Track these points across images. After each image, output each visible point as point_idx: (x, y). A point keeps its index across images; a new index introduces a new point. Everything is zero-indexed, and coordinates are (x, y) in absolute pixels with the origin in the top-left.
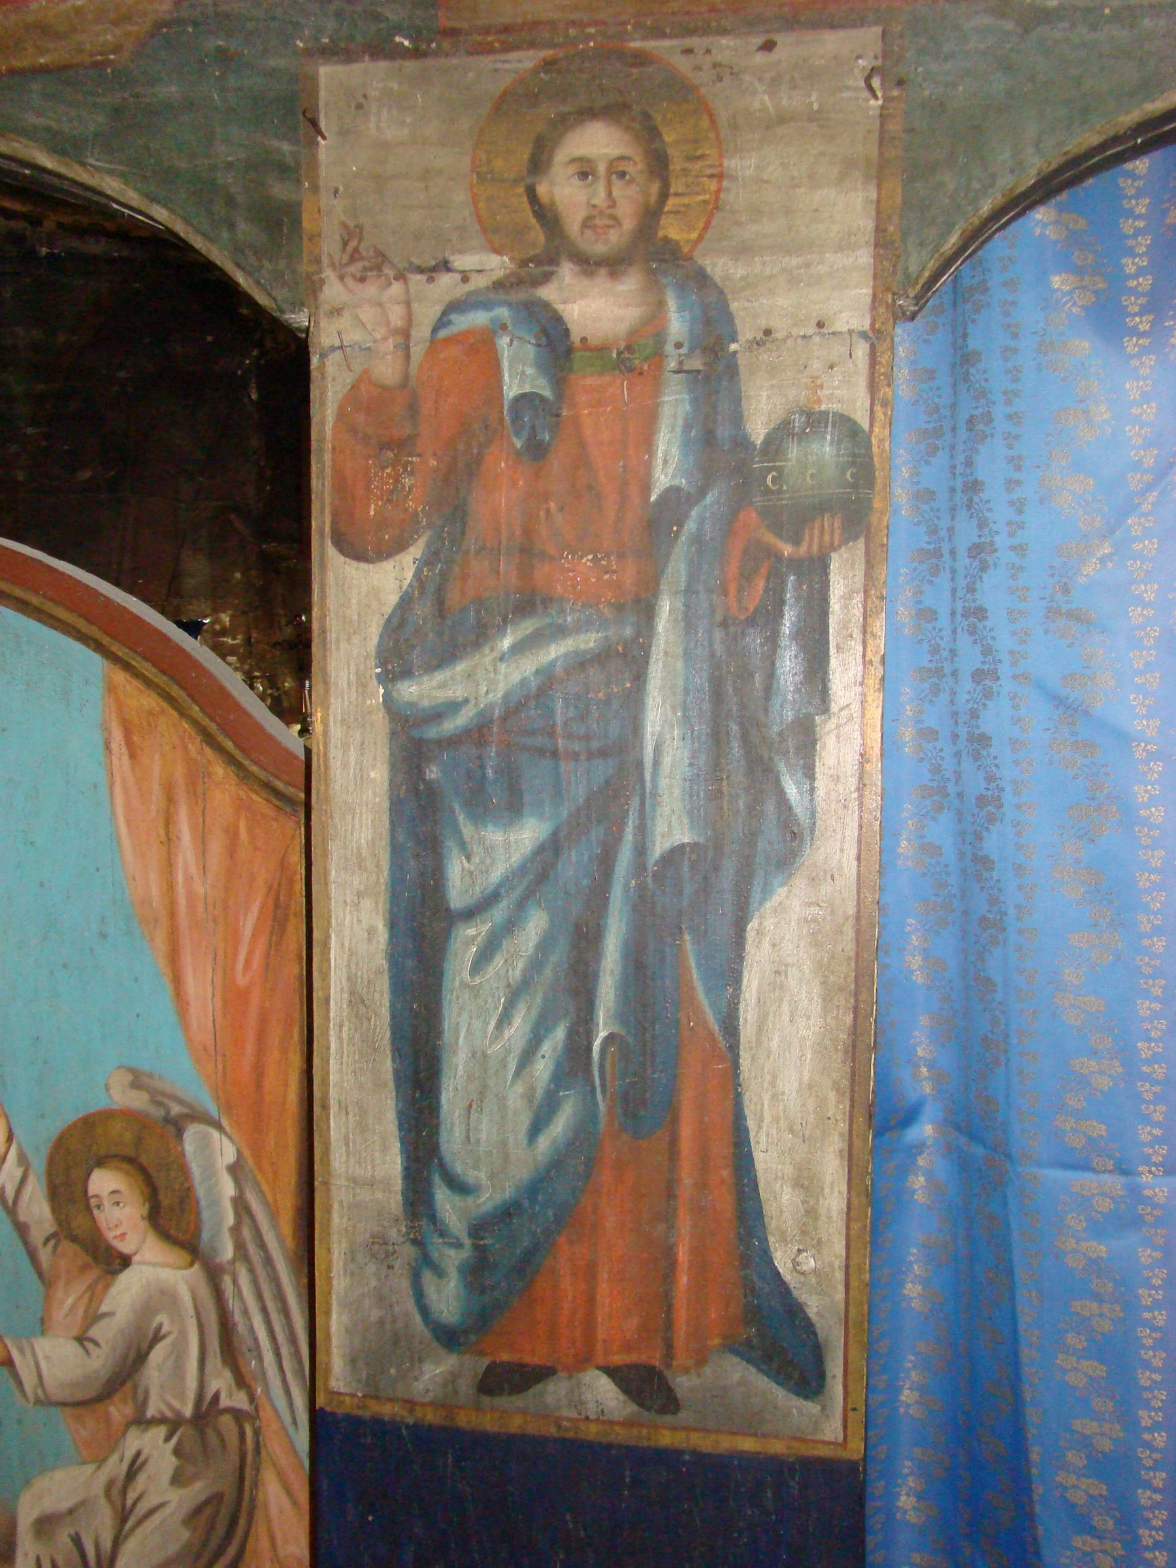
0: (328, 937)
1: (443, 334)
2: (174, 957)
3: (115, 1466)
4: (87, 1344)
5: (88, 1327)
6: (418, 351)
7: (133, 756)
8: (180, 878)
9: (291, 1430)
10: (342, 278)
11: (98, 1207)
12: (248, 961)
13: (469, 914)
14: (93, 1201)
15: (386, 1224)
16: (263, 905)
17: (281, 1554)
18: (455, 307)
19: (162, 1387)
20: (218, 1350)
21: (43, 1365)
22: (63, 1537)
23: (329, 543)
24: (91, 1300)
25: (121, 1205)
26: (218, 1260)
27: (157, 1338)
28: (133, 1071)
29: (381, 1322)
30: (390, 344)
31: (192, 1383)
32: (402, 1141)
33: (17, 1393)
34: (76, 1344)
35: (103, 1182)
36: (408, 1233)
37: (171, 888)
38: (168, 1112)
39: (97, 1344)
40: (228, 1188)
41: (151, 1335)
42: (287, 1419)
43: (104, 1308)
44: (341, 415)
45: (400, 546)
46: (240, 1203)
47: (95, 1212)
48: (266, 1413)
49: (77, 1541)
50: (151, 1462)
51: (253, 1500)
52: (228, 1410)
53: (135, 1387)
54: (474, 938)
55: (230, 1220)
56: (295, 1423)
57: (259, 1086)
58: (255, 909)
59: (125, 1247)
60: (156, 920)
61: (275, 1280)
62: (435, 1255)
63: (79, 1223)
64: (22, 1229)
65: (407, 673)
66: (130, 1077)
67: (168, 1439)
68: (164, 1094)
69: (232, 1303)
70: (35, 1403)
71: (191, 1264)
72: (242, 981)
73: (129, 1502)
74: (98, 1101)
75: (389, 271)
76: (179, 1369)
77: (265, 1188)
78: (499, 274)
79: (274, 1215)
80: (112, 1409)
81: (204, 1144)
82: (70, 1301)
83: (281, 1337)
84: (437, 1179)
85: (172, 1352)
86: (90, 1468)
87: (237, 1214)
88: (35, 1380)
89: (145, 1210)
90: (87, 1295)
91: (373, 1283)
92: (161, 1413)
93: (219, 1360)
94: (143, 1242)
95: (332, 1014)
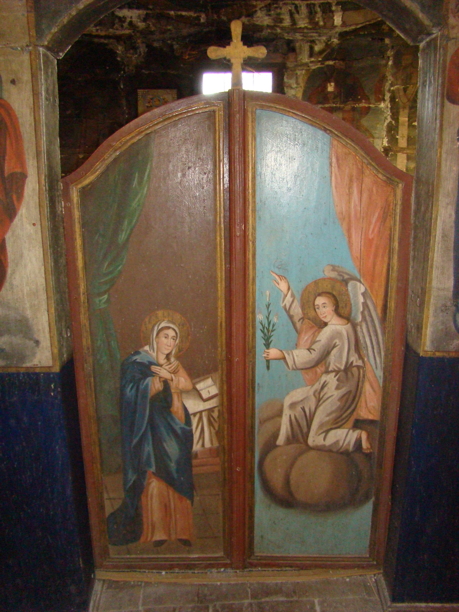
0: (437, 217)
2: (349, 230)
3: (317, 386)
4: (311, 350)
5: (311, 346)
7: (339, 167)
8: (353, 205)
9: (375, 370)
11: (318, 308)
14: (316, 307)
15: (447, 301)
16: (379, 214)
17: (368, 406)
24: (313, 337)
26: (356, 322)
27: (334, 346)
28: (333, 266)
31: (344, 359)
32: (454, 276)
33: (286, 367)
34: (307, 351)
35: (320, 301)
36: (453, 303)
37: (350, 208)
38: (343, 277)
39: (314, 350)
40: (361, 300)
41: (333, 345)
43: (318, 339)
46: (365, 305)
47: (317, 310)
48: (368, 366)
49: (303, 409)
52: (355, 366)
53: (326, 363)
55: (361, 309)
56: (376, 368)
57: (374, 268)
58: (376, 215)
59: (325, 320)
60: (344, 219)
61: (374, 326)
63: (312, 314)
64: (291, 317)
66: (331, 268)
67: (335, 377)
68: (343, 272)
69: (360, 335)
70: (292, 370)
71: (348, 324)
72: (371, 237)
73: (321, 396)
74: (320, 275)
76: (341, 356)
77: (373, 299)
80: (318, 369)
81: (355, 287)
83: (374, 343)
86: (309, 387)
87: (363, 307)
88: (293, 363)
89: (333, 309)
90: (312, 336)
91: (441, 318)
95: (436, 240)
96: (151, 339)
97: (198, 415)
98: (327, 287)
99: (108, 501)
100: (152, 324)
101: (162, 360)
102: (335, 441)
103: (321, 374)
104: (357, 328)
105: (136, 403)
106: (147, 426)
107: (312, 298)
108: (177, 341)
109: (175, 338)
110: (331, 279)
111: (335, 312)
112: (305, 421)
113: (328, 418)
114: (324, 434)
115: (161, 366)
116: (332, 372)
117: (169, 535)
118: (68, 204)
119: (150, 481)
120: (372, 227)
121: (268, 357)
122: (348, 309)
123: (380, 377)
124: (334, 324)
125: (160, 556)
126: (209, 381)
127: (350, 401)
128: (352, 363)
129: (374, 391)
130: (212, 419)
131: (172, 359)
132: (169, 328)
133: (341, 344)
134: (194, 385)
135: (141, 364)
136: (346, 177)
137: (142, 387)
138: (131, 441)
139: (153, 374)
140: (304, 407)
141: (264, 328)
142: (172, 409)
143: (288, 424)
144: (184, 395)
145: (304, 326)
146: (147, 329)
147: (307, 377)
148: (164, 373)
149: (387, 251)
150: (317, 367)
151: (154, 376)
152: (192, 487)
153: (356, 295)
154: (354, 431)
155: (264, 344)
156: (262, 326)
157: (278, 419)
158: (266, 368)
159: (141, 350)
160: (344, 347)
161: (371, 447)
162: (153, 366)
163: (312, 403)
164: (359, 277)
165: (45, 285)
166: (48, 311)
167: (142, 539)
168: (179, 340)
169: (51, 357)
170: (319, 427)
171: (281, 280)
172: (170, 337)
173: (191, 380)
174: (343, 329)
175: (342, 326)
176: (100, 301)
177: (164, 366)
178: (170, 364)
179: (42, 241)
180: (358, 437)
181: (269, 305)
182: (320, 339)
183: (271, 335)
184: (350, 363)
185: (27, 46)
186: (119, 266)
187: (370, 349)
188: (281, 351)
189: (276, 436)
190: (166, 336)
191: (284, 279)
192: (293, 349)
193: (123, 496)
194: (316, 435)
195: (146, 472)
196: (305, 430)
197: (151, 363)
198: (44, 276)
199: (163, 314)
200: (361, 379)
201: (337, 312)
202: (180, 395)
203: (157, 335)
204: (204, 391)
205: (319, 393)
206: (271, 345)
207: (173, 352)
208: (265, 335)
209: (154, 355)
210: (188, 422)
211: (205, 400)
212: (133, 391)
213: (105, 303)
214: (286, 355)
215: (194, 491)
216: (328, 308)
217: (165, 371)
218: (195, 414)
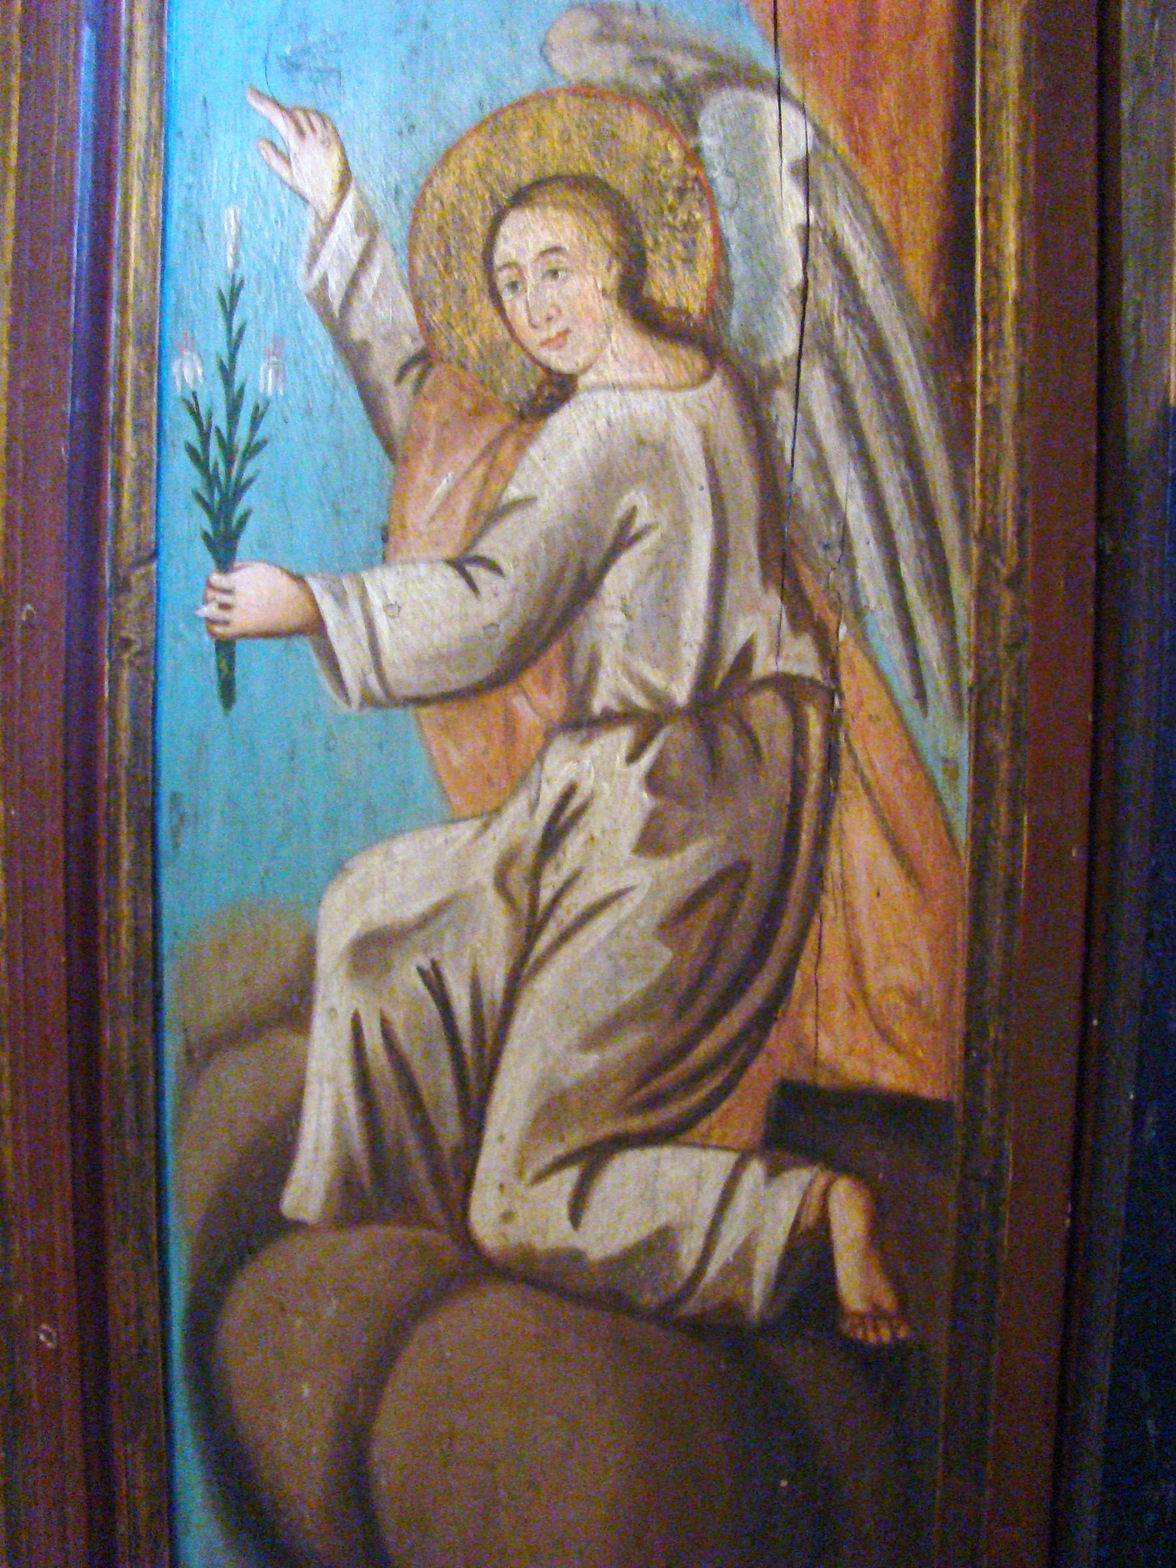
4: (471, 569)
9: (911, 711)
11: (513, 286)
14: (503, 278)
17: (873, 985)
19: (629, 645)
20: (755, 561)
21: (382, 623)
25: (561, 274)
26: (764, 361)
27: (624, 539)
34: (451, 573)
38: (669, 77)
39: (494, 568)
42: (904, 688)
43: (514, 492)
47: (507, 297)
49: (434, 981)
50: (599, 805)
56: (921, 695)
59: (559, 361)
66: (594, 22)
67: (632, 758)
70: (362, 705)
71: (706, 377)
73: (546, 895)
77: (874, 194)
82: (443, 486)
83: (897, 509)
85: (651, 570)
86: (465, 831)
88: (366, 656)
90: (480, 471)
92: (624, 700)
93: (755, 578)
103: (539, 739)
104: (769, 400)
110: (585, 91)
111: (621, 304)
112: (445, 1063)
113: (591, 1061)
114: (570, 1176)
116: (610, 720)
121: (226, 623)
122: (704, 271)
124: (615, 386)
127: (738, 946)
128: (746, 654)
129: (912, 872)
133: (664, 519)
140: (435, 965)
141: (205, 436)
143: (347, 1076)
145: (433, 409)
150: (509, 690)
154: (774, 1172)
155: (206, 536)
156: (199, 424)
157: (284, 1039)
158: (214, 690)
160: (685, 544)
161: (902, 1304)
164: (768, 64)
170: (536, 1120)
171: (301, 133)
174: (679, 414)
175: (670, 396)
180: (809, 1219)
181: (235, 292)
182: (528, 490)
183: (245, 477)
184: (729, 657)
187: (867, 552)
188: (299, 579)
191: (318, 125)
192: (370, 566)
194: (520, 1174)
196: (450, 1130)
200: (814, 780)
205: (535, 876)
206: (244, 545)
208: (211, 479)
214: (328, 608)
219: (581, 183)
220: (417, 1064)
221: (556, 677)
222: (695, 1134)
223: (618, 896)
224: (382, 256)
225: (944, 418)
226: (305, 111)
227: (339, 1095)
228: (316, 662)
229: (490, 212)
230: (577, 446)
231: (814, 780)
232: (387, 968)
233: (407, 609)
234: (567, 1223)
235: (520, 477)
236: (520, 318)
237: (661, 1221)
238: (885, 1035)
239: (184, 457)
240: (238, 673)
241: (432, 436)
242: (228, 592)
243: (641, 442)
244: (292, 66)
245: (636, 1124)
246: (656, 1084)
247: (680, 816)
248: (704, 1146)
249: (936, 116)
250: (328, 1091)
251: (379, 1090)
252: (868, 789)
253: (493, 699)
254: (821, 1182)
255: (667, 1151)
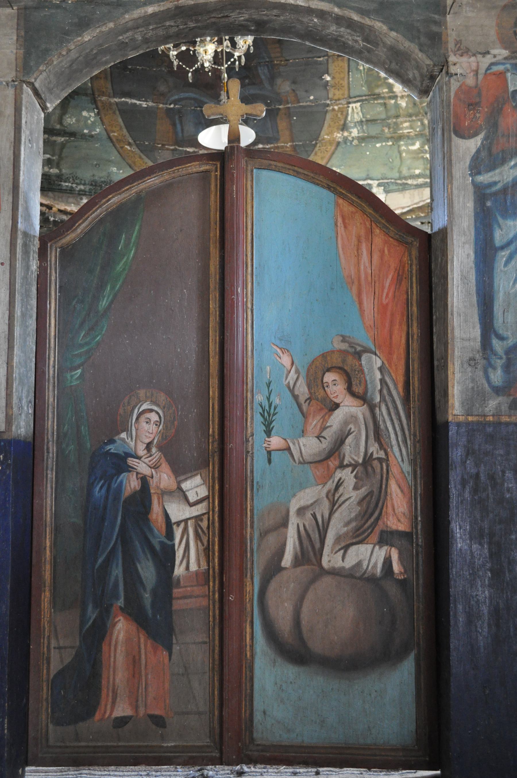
0: (453, 257)
1: (489, 72)
3: (331, 485)
4: (320, 438)
5: (321, 433)
6: (481, 77)
7: (345, 227)
8: (362, 268)
9: (401, 463)
10: (455, 55)
11: (327, 386)
12: (387, 295)
13: (502, 248)
14: (325, 385)
15: (475, 353)
17: (396, 511)
18: (492, 64)
19: (351, 453)
21: (303, 448)
22: (308, 515)
23: (452, 133)
26: (374, 402)
27: (349, 433)
28: (342, 336)
29: (473, 388)
30: (472, 74)
32: (480, 324)
33: (291, 460)
34: (316, 439)
35: (329, 377)
36: (483, 356)
37: (359, 271)
38: (355, 349)
39: (325, 438)
40: (378, 376)
41: (347, 432)
42: (400, 460)
43: (328, 424)
44: (456, 94)
45: (476, 134)
46: (383, 381)
47: (326, 388)
49: (314, 516)
50: (345, 481)
51: (386, 492)
52: (375, 459)
53: (339, 455)
54: (504, 256)
57: (391, 338)
58: (390, 277)
59: (337, 401)
60: (353, 283)
61: (396, 408)
62: (493, 362)
63: (320, 394)
64: (296, 397)
65: (479, 173)
66: (341, 338)
67: (352, 472)
69: (379, 418)
70: (299, 464)
71: (364, 405)
72: (385, 302)
73: (336, 498)
74: (329, 348)
75: (470, 53)
76: (357, 445)
77: (393, 374)
78: (506, 55)
79: (396, 385)
81: (370, 361)
82: (315, 422)
83: (398, 429)
84: (493, 336)
86: (320, 487)
88: (299, 454)
90: (322, 420)
91: (470, 374)
92: (350, 462)
94: (345, 397)
95: (455, 283)
96: (130, 424)
97: (182, 525)
98: (336, 360)
99: (57, 650)
100: (132, 406)
101: (141, 451)
102: (357, 561)
103: (334, 470)
105: (105, 508)
106: (117, 539)
107: (320, 374)
108: (161, 427)
109: (158, 424)
110: (340, 351)
112: (317, 533)
113: (346, 529)
114: (342, 552)
115: (139, 458)
116: (347, 466)
117: (136, 708)
118: (44, 264)
119: (117, 620)
120: (386, 291)
121: (269, 448)
123: (408, 472)
125: (120, 744)
126: (198, 479)
127: (372, 506)
129: (402, 491)
130: (200, 530)
131: (154, 450)
132: (151, 411)
133: (357, 430)
134: (179, 483)
135: (116, 455)
136: (354, 237)
137: (114, 486)
138: (96, 561)
139: (129, 469)
140: (314, 513)
141: (264, 411)
142: (149, 516)
143: (296, 536)
144: (166, 497)
145: (312, 408)
146: (125, 412)
147: (318, 473)
148: (143, 468)
149: (405, 318)
150: (329, 460)
151: (130, 471)
152: (170, 630)
153: (371, 369)
154: (380, 547)
156: (262, 408)
157: (282, 530)
158: (266, 461)
159: (116, 438)
162: (130, 459)
163: (325, 507)
164: (374, 349)
165: (7, 333)
166: (7, 364)
167: (97, 716)
168: (163, 426)
169: (4, 420)
171: (283, 353)
172: (152, 422)
173: (176, 478)
176: (72, 376)
177: (143, 459)
178: (151, 456)
179: (10, 283)
180: (387, 556)
181: (270, 383)
182: (332, 424)
184: (369, 455)
185: (13, 81)
186: (97, 336)
187: (393, 436)
188: (285, 440)
189: (280, 553)
190: (148, 420)
192: (300, 437)
193: (78, 644)
194: (332, 553)
195: (112, 605)
196: (318, 545)
197: (128, 455)
198: (7, 322)
199: (146, 395)
200: (385, 476)
201: (350, 390)
202: (160, 496)
203: (137, 419)
204: (190, 491)
205: (334, 495)
206: (273, 433)
207: (155, 441)
208: (265, 420)
209: (132, 444)
210: (170, 535)
211: (191, 505)
212: (104, 491)
213: (77, 379)
214: (291, 445)
215: (174, 637)
216: (339, 387)
217: (144, 465)
218: (178, 523)
219: (340, 368)
220: (311, 532)
221: (337, 458)
222: (366, 542)
223: (350, 498)
224: (301, 379)
225: (405, 414)
226: (284, 349)
227: (294, 540)
228: (289, 455)
229: (322, 372)
230: (340, 416)
231: (385, 476)
232: (304, 514)
233: (308, 446)
234: (341, 561)
235: (329, 421)
236: (329, 393)
237: (360, 559)
238: (399, 520)
239: (259, 415)
240: (272, 458)
241: (312, 413)
242: (270, 442)
243: (352, 416)
244: (281, 340)
245: (354, 541)
246: (358, 533)
247: (361, 483)
248: (367, 544)
249: (403, 362)
250: (292, 539)
251: (303, 538)
252: (394, 477)
253: (325, 462)
254: (389, 549)
255: (360, 545)
